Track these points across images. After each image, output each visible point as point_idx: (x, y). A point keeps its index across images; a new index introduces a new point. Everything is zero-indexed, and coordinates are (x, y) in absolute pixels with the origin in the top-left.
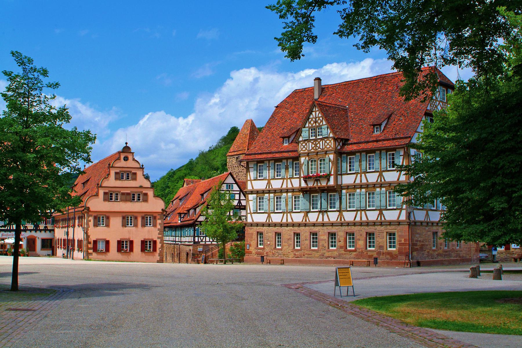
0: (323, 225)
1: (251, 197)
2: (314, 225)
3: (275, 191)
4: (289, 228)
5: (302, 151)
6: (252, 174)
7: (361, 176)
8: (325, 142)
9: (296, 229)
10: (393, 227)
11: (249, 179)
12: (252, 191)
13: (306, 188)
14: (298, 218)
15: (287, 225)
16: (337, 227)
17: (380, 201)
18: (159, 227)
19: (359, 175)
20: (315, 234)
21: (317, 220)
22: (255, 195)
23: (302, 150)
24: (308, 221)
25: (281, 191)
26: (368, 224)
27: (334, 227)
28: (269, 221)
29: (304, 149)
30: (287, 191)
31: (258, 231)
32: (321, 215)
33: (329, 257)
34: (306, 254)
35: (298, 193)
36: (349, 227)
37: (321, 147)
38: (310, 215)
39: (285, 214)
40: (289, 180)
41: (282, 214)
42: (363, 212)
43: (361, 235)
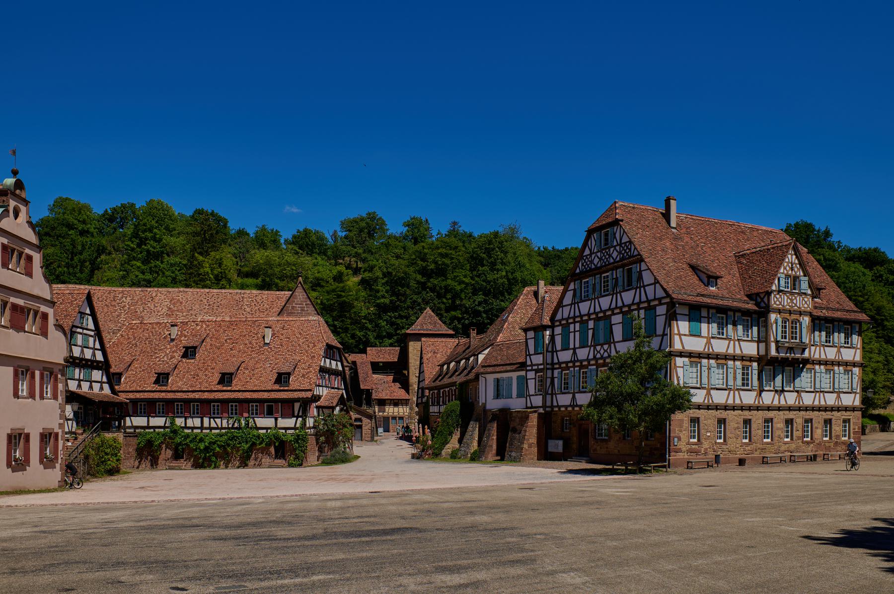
0: (779, 409)
1: (679, 361)
2: (768, 408)
3: (717, 357)
4: (737, 412)
5: (775, 305)
6: (683, 326)
7: (820, 350)
8: (803, 299)
9: (747, 414)
10: (848, 413)
11: (676, 332)
12: (681, 352)
13: (777, 358)
14: (749, 398)
15: (734, 408)
16: (795, 412)
17: (821, 382)
18: (60, 398)
19: (818, 348)
20: (769, 421)
21: (772, 402)
22: (686, 360)
23: (775, 303)
24: (761, 403)
25: (726, 357)
26: (826, 409)
27: (791, 412)
28: (708, 401)
29: (778, 303)
30: (734, 358)
31: (692, 416)
32: (777, 397)
33: (786, 451)
34: (759, 449)
35: (748, 363)
36: (808, 412)
37: (798, 305)
38: (764, 394)
39: (732, 392)
40: (737, 343)
41: (727, 392)
42: (822, 394)
43: (819, 422)
